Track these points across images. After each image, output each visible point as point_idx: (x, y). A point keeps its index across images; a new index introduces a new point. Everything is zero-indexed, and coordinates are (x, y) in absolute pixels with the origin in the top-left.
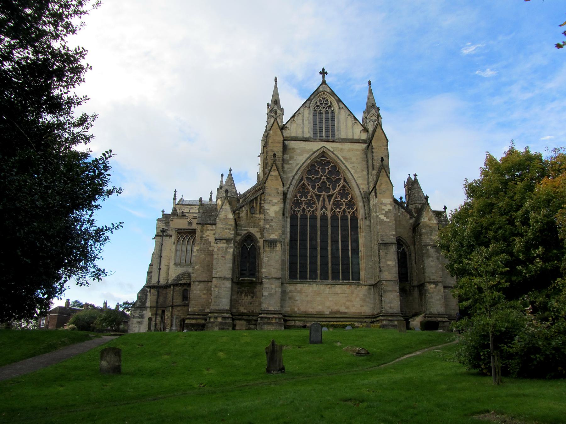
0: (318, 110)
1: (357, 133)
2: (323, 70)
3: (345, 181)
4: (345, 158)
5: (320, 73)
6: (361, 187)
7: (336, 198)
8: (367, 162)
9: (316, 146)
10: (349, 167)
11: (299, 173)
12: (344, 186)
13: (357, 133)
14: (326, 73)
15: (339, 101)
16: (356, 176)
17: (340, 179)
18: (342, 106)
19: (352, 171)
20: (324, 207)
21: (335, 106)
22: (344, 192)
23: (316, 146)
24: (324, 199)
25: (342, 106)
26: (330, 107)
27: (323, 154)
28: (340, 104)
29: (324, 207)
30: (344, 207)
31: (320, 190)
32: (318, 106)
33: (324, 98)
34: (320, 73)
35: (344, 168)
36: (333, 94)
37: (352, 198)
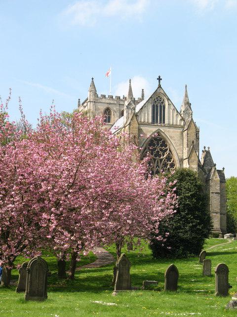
0: (155, 105)
1: (178, 121)
2: (159, 77)
3: (170, 151)
4: (171, 137)
5: (158, 79)
6: (179, 155)
7: (164, 161)
8: (183, 140)
9: (154, 129)
10: (173, 142)
11: (145, 145)
12: (169, 154)
13: (178, 121)
14: (161, 79)
15: (168, 99)
16: (176, 148)
17: (167, 149)
18: (170, 103)
19: (174, 145)
20: (157, 166)
21: (166, 103)
22: (169, 158)
23: (154, 129)
24: (158, 161)
25: (170, 103)
26: (162, 102)
27: (159, 133)
28: (169, 101)
29: (157, 166)
30: (168, 166)
31: (156, 156)
32: (156, 102)
33: (159, 97)
34: (158, 79)
35: (170, 143)
36: (165, 95)
37: (173, 161)
